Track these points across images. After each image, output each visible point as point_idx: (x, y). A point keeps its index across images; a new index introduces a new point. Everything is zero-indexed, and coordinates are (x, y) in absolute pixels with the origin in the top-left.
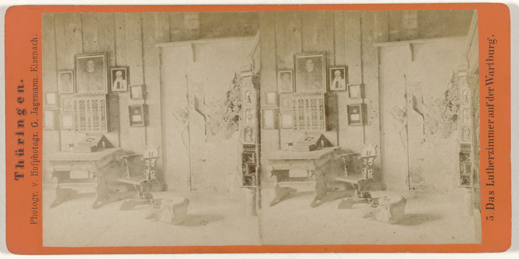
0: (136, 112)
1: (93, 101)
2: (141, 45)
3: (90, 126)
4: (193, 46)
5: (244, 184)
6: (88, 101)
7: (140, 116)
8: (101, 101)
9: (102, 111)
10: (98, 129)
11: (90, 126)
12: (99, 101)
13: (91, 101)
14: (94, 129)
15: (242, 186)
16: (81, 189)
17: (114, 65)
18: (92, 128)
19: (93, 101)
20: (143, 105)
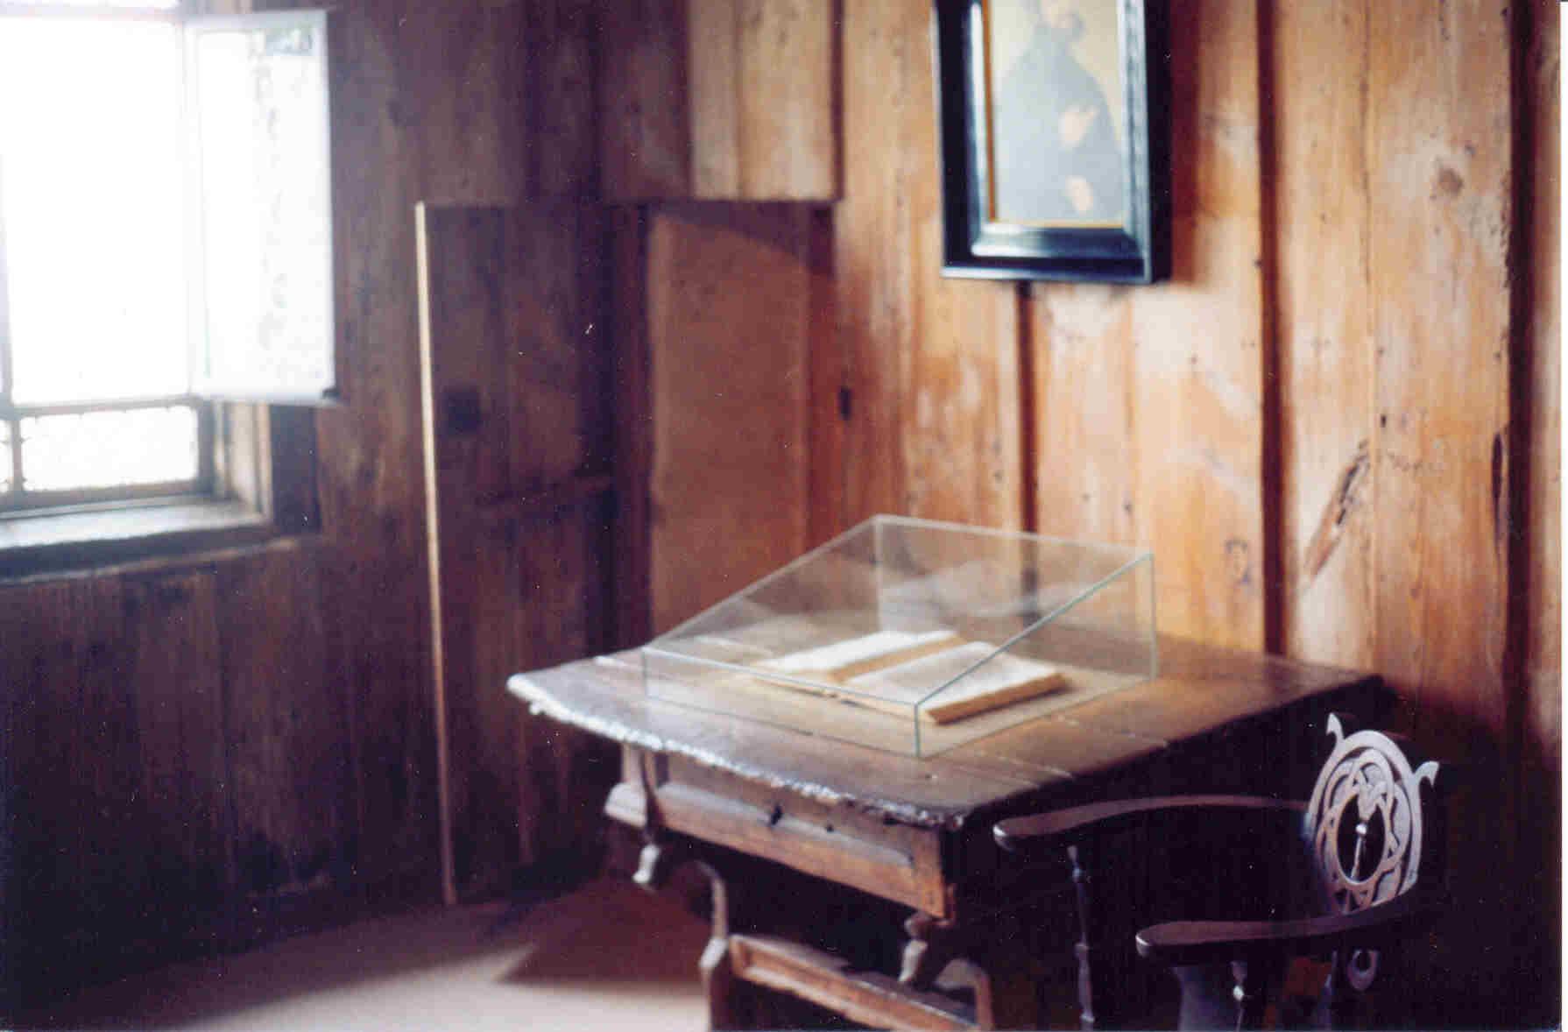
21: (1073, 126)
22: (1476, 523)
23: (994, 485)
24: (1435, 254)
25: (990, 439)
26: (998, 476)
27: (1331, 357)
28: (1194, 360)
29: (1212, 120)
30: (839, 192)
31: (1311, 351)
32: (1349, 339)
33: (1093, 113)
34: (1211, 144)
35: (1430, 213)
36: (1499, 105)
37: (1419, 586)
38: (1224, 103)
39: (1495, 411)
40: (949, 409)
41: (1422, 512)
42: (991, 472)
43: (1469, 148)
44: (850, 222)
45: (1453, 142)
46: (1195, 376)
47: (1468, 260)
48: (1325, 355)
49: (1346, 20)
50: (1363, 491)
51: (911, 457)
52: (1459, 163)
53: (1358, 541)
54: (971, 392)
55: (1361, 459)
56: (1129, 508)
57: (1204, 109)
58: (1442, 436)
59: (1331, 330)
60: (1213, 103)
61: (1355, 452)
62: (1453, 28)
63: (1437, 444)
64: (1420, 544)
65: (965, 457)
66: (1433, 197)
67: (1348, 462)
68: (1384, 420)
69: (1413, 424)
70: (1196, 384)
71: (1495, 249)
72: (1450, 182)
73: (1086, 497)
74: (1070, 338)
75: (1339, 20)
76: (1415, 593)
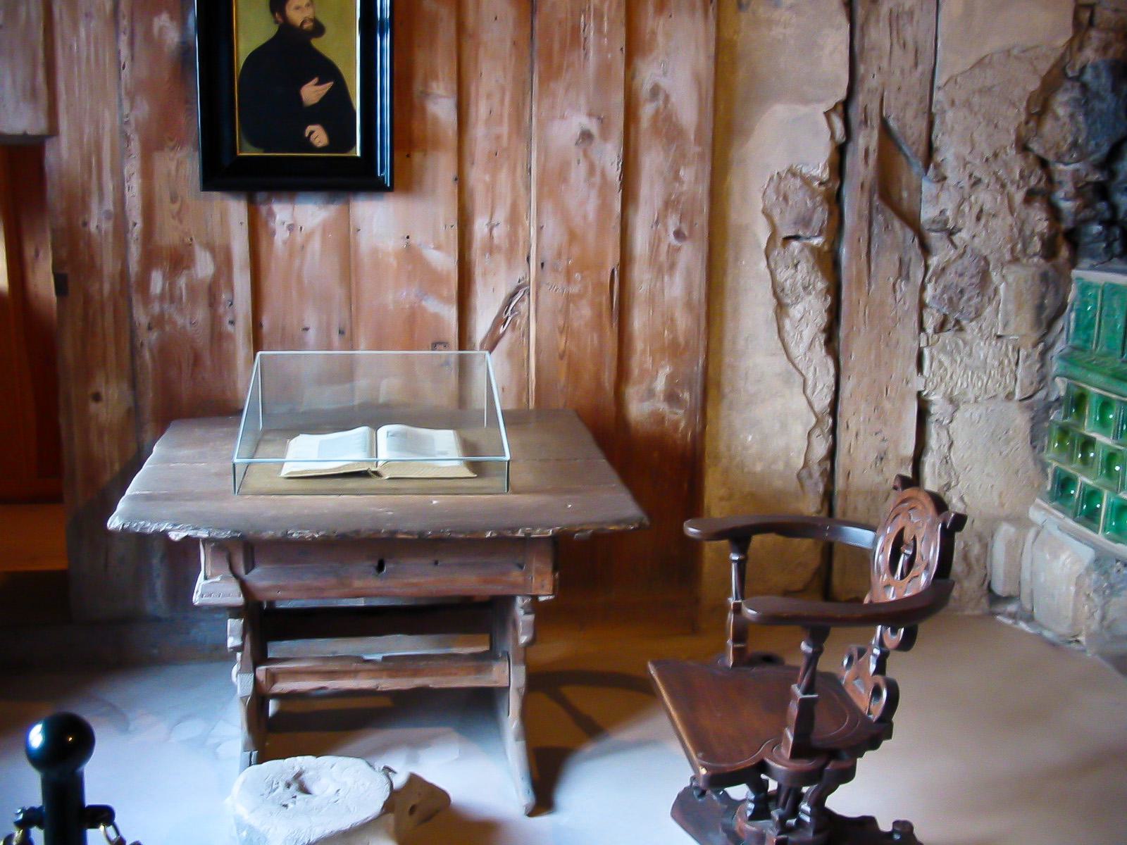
21: (312, 93)
22: (600, 315)
23: (230, 328)
24: (578, 173)
25: (224, 297)
26: (232, 323)
27: (500, 233)
28: (408, 237)
29: (426, 94)
30: (53, 131)
31: (486, 230)
32: (514, 219)
33: (329, 85)
34: (423, 109)
35: (574, 153)
36: (618, 98)
37: (564, 352)
38: (434, 85)
39: (612, 259)
40: (182, 282)
41: (566, 313)
42: (227, 319)
43: (599, 118)
44: (62, 155)
45: (590, 115)
46: (408, 245)
47: (597, 179)
48: (496, 232)
49: (514, 43)
50: (527, 307)
51: (141, 317)
52: (593, 127)
53: (517, 333)
54: (204, 267)
55: (519, 288)
56: (341, 332)
57: (418, 87)
58: (581, 272)
59: (501, 216)
60: (426, 84)
61: (516, 283)
62: (591, 54)
63: (577, 276)
64: (565, 330)
65: (201, 314)
66: (577, 144)
67: (511, 289)
68: (542, 264)
69: (562, 265)
70: (411, 254)
71: (614, 172)
72: (586, 136)
73: (307, 329)
74: (291, 228)
75: (508, 44)
76: (562, 357)
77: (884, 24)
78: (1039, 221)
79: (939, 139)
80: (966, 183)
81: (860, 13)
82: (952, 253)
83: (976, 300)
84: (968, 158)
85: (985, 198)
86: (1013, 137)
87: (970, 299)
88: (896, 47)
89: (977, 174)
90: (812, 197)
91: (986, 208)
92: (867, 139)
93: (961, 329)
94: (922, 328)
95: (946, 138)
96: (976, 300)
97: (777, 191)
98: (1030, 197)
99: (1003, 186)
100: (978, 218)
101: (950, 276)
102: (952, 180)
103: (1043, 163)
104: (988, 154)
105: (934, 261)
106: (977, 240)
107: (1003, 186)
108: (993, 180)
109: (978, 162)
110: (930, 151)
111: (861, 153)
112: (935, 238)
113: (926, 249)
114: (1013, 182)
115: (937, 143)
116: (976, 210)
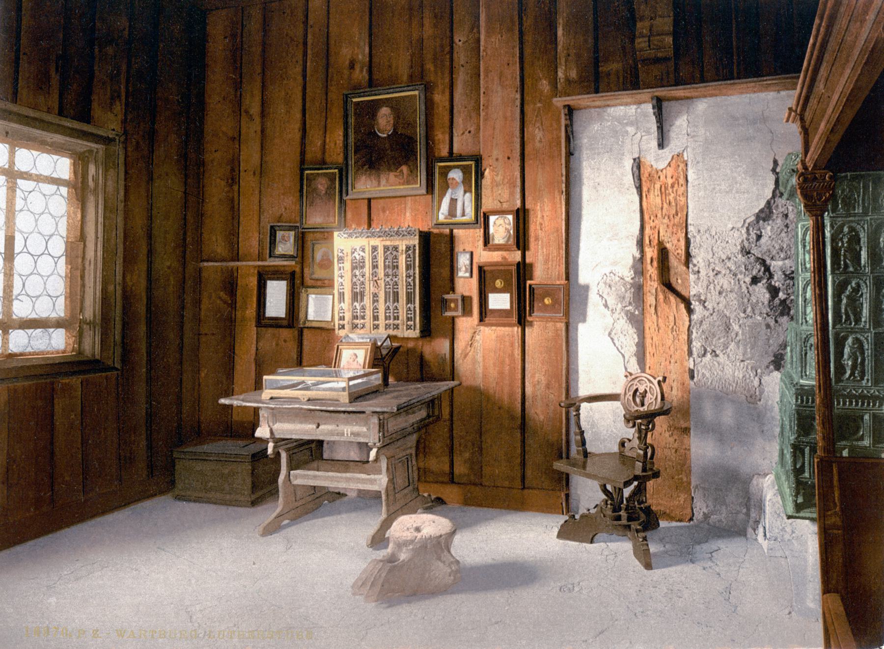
0: (499, 283)
1: (386, 248)
2: (518, 103)
3: (376, 318)
4: (659, 105)
5: (799, 507)
6: (375, 249)
7: (507, 296)
8: (408, 248)
9: (408, 276)
10: (397, 327)
11: (376, 318)
12: (402, 247)
13: (381, 250)
14: (387, 327)
15: (790, 509)
16: (350, 482)
17: (445, 152)
18: (382, 322)
19: (386, 248)
20: (518, 264)
77: (657, 192)
78: (761, 292)
79: (693, 251)
80: (711, 274)
81: (645, 189)
82: (707, 313)
83: (722, 340)
84: (711, 260)
85: (725, 282)
86: (739, 248)
87: (719, 339)
88: (665, 206)
89: (717, 268)
90: (624, 285)
91: (725, 286)
92: (651, 253)
93: (717, 356)
94: (690, 353)
95: (697, 251)
96: (722, 340)
97: (605, 283)
98: (755, 280)
99: (735, 275)
100: (720, 293)
101: (705, 326)
102: (703, 273)
103: (763, 262)
104: (724, 257)
105: (694, 317)
106: (720, 305)
107: (735, 275)
108: (728, 272)
109: (717, 262)
110: (688, 256)
111: (649, 261)
112: (695, 304)
113: (690, 311)
114: (741, 273)
115: (693, 254)
116: (718, 288)
